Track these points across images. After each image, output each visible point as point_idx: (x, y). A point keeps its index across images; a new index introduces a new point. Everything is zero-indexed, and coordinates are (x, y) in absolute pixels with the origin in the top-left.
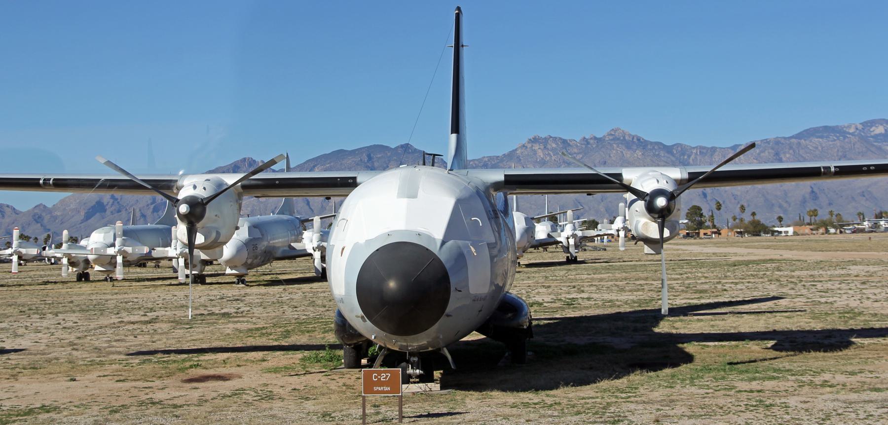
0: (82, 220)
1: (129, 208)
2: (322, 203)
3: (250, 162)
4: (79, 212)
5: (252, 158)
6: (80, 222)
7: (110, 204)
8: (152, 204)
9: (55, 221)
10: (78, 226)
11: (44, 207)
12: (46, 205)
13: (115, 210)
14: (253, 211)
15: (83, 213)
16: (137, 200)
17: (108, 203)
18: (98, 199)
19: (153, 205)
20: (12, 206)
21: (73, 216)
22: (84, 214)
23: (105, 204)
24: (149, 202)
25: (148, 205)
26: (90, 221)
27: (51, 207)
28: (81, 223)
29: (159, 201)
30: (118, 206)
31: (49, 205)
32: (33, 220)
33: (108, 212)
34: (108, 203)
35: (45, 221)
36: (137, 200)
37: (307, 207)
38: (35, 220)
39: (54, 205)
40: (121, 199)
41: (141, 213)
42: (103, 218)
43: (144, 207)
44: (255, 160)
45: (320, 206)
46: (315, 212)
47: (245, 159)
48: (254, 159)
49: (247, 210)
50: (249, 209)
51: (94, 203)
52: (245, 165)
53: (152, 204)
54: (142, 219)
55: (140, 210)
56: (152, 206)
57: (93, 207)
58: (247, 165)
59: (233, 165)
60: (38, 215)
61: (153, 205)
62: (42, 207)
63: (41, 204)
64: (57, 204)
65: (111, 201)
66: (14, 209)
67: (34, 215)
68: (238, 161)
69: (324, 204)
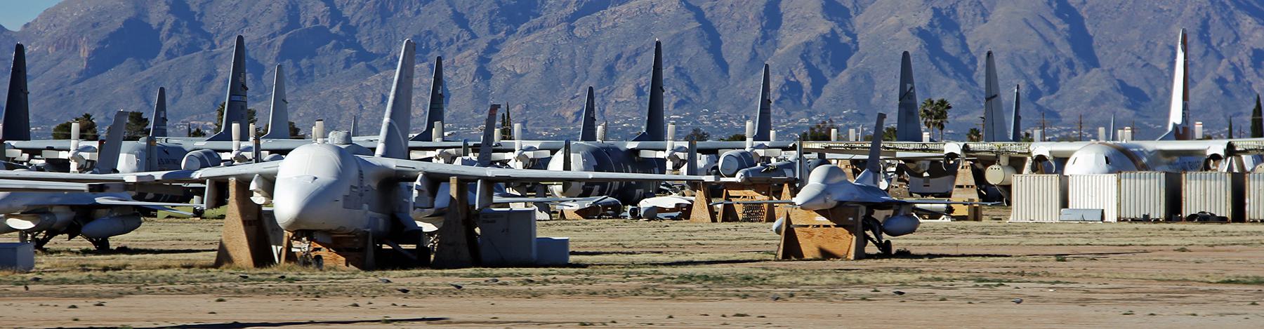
1: (221, 42)
2: (753, 49)
4: (76, 47)
6: (74, 77)
7: (167, 27)
10: (67, 90)
13: (180, 45)
15: (84, 52)
18: (132, 14)
21: (59, 60)
22: (86, 55)
24: (277, 27)
26: (107, 77)
28: (76, 82)
29: (308, 25)
36: (245, 21)
37: (707, 60)
39: (27, 25)
45: (746, 55)
46: (731, 72)
49: (534, 59)
51: (118, 23)
56: (280, 40)
64: (36, 21)
65: (171, 20)
69: (760, 51)
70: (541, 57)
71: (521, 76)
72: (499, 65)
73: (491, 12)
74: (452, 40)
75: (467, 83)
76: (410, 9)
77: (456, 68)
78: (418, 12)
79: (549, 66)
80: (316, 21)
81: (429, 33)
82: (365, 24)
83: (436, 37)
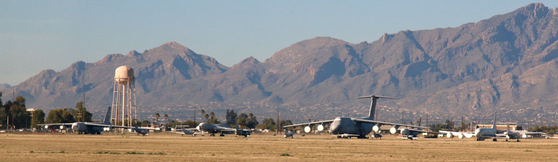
0: (311, 82)
3: (540, 10)
5: (542, 5)
6: (309, 84)
7: (349, 61)
8: (404, 64)
9: (275, 81)
11: (254, 63)
12: (258, 59)
14: (549, 79)
15: (312, 72)
16: (384, 58)
17: (345, 60)
19: (407, 66)
20: (214, 59)
21: (299, 76)
22: (314, 74)
23: (342, 61)
24: (401, 61)
25: (399, 66)
26: (321, 85)
27: (263, 62)
30: (359, 65)
31: (262, 59)
32: (247, 79)
33: (347, 74)
34: (345, 60)
35: (263, 81)
38: (250, 79)
39: (268, 60)
40: (362, 55)
41: (391, 76)
42: (339, 81)
43: (393, 67)
44: (547, 8)
47: (533, 5)
48: (546, 6)
49: (540, 78)
50: (544, 76)
51: (326, 60)
52: (533, 14)
53: (404, 64)
54: (393, 85)
55: (390, 72)
57: (326, 65)
58: (535, 14)
59: (516, 14)
60: (253, 72)
61: (407, 66)
62: (252, 62)
63: (252, 57)
64: (272, 58)
66: (217, 63)
67: (249, 73)
68: (524, 8)
70: (544, 76)
71: (534, 85)
72: (523, 80)
73: (501, 55)
74: (484, 68)
75: (508, 89)
76: (462, 53)
77: (502, 81)
78: (466, 55)
79: (548, 81)
80: (418, 59)
81: (473, 64)
82: (441, 60)
83: (477, 66)
